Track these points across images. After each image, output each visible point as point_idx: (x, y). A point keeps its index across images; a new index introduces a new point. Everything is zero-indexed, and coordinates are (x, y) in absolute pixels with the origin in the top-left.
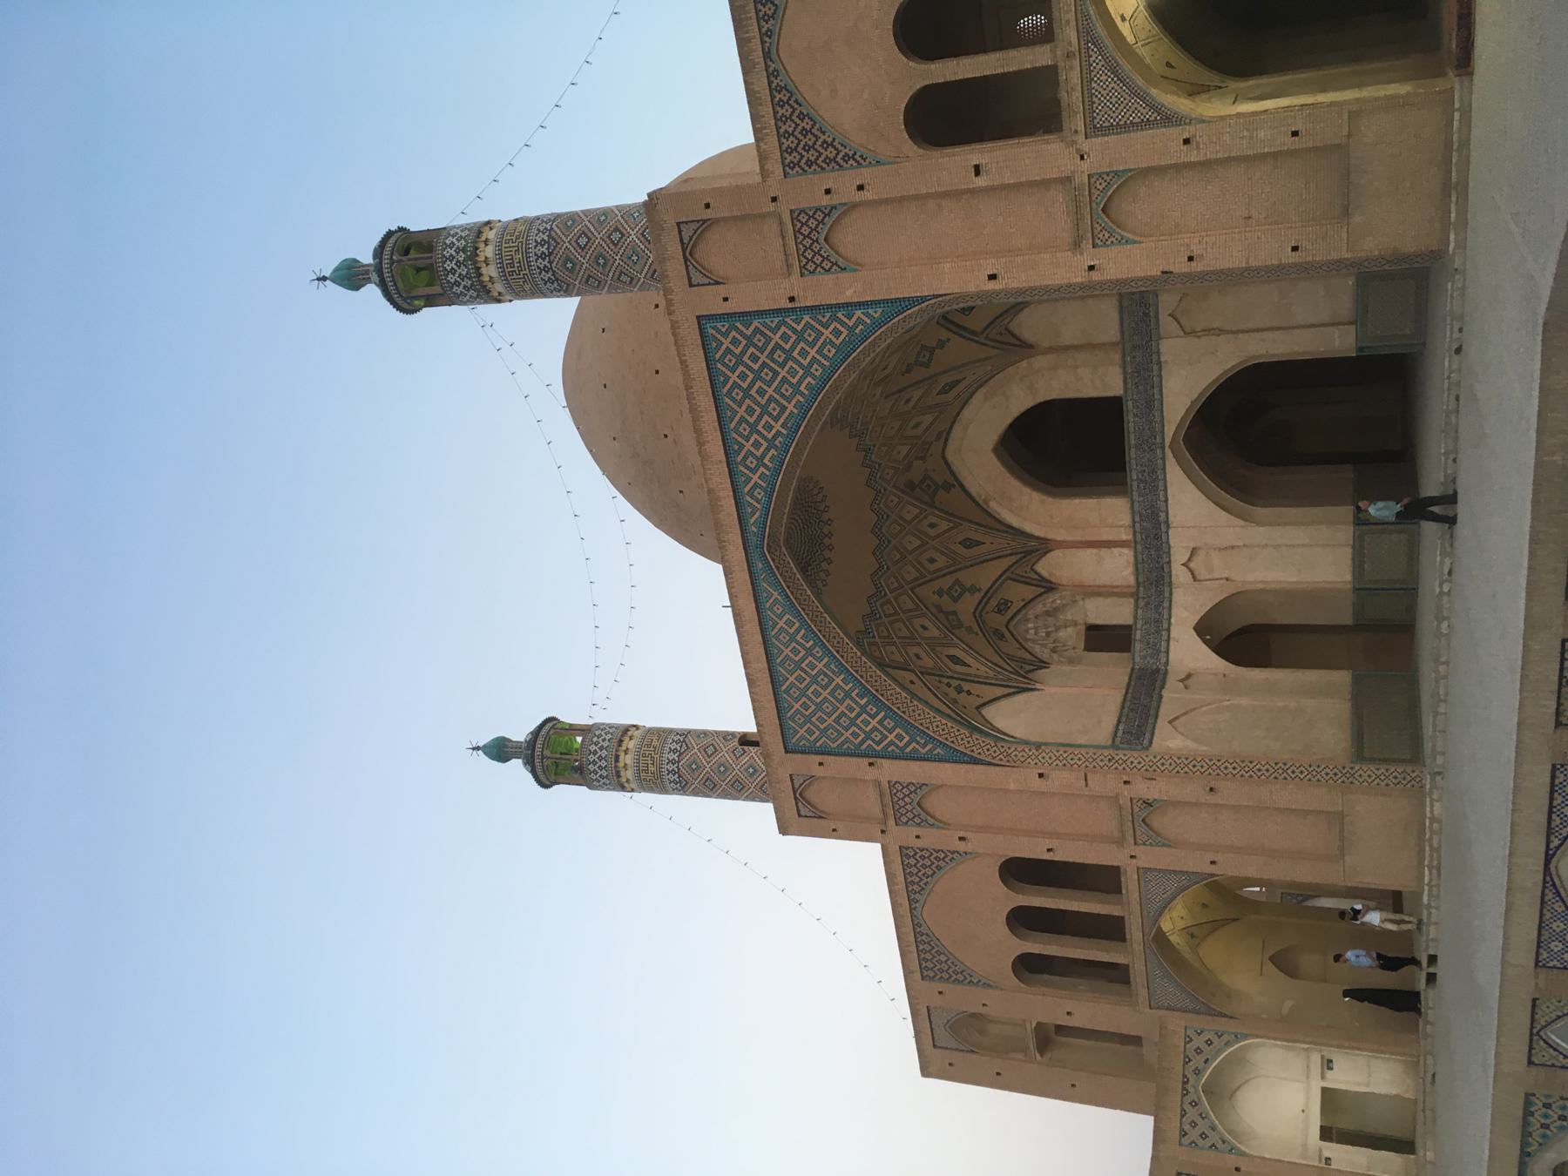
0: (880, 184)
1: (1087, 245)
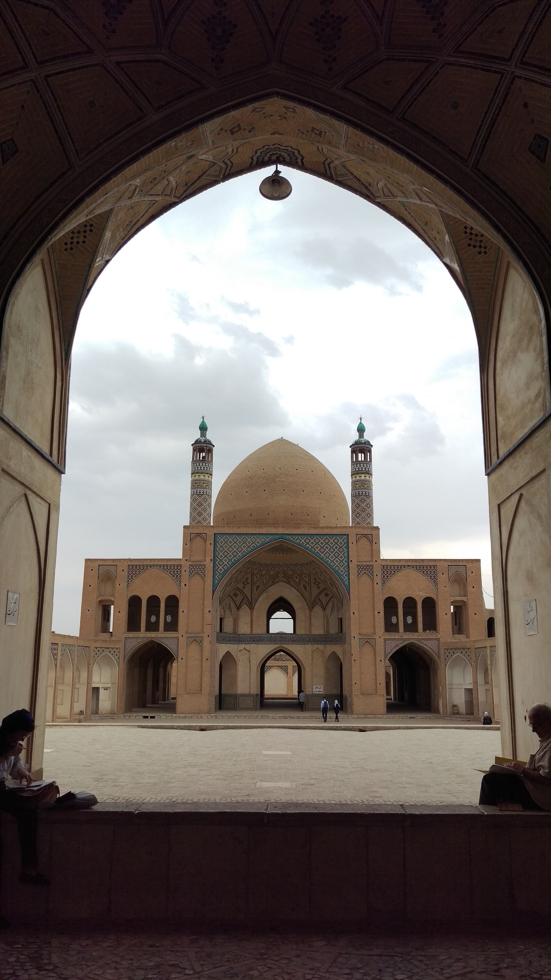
0: (378, 588)
1: (360, 637)
